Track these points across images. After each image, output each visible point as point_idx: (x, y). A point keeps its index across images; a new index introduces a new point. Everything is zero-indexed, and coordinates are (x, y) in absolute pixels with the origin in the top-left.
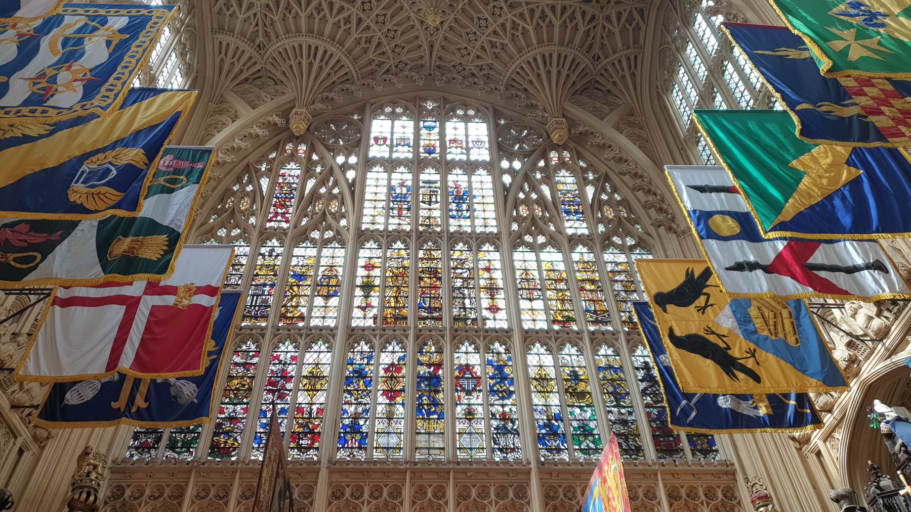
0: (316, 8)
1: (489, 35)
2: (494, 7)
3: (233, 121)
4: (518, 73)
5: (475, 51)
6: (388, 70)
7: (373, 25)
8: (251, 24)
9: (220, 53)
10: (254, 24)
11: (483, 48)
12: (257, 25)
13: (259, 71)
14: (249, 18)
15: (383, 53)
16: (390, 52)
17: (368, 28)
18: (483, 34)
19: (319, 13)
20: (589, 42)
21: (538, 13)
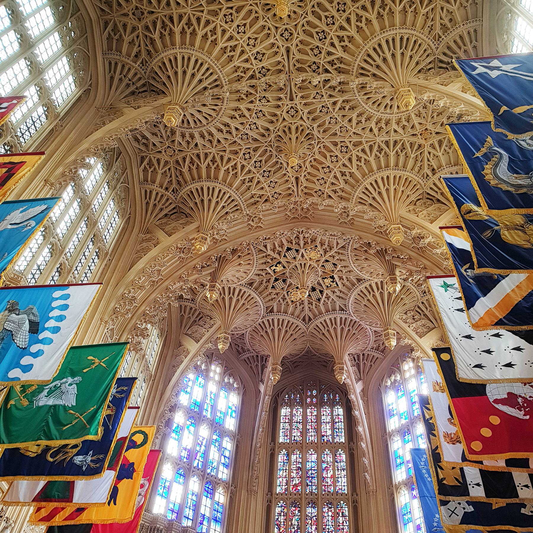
0: (211, 161)
2: (342, 146)
3: (155, 246)
4: (363, 192)
5: (329, 180)
6: (266, 200)
7: (253, 169)
8: (167, 176)
9: (146, 198)
10: (169, 176)
11: (335, 177)
12: (171, 176)
13: (174, 208)
14: (165, 172)
15: (262, 188)
16: (267, 187)
17: (249, 171)
18: (335, 167)
19: (213, 164)
21: (376, 148)
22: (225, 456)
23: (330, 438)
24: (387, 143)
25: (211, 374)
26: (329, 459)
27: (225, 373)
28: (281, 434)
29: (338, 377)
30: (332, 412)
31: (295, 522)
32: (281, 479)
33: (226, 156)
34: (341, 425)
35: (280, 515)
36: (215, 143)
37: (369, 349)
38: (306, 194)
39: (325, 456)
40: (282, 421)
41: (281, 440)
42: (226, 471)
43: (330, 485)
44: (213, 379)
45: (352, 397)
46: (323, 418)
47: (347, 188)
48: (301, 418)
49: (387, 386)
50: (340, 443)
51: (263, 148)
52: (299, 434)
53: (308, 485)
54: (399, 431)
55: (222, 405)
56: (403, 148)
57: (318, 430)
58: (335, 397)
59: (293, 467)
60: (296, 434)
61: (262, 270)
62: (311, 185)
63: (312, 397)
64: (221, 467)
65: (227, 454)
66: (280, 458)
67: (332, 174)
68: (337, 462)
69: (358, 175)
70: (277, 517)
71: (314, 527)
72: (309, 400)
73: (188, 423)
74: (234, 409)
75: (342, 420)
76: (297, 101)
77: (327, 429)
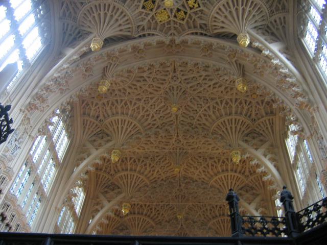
1: (202, 111)
3: (88, 157)
6: (158, 127)
12: (99, 112)
20: (249, 113)
24: (231, 100)
33: (134, 102)
36: (127, 94)
38: (182, 124)
47: (207, 124)
51: (156, 98)
56: (241, 103)
61: (148, 141)
62: (185, 120)
67: (198, 115)
69: (214, 117)
76: (178, 73)
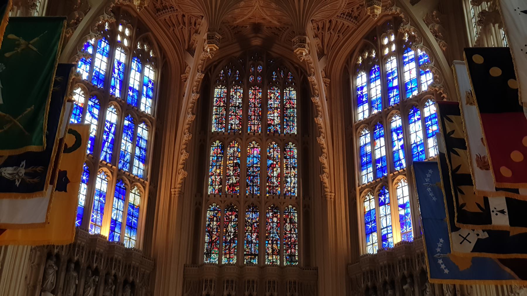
22: (140, 148)
23: (278, 128)
25: (119, 38)
26: (277, 154)
27: (137, 35)
28: (214, 121)
29: (297, 51)
30: (282, 95)
31: (231, 229)
32: (213, 177)
34: (293, 112)
35: (211, 220)
37: (339, 15)
39: (272, 150)
40: (215, 104)
41: (213, 129)
42: (142, 165)
43: (277, 186)
44: (121, 44)
45: (313, 79)
46: (270, 102)
48: (240, 101)
49: (356, 65)
50: (290, 135)
52: (237, 122)
53: (248, 185)
54: (368, 124)
55: (134, 80)
57: (263, 118)
58: (286, 75)
59: (230, 163)
60: (234, 122)
63: (256, 74)
64: (136, 162)
65: (143, 144)
66: (212, 152)
68: (286, 158)
70: (208, 223)
71: (254, 236)
72: (251, 78)
73: (90, 103)
74: (150, 85)
75: (295, 106)
77: (274, 117)
